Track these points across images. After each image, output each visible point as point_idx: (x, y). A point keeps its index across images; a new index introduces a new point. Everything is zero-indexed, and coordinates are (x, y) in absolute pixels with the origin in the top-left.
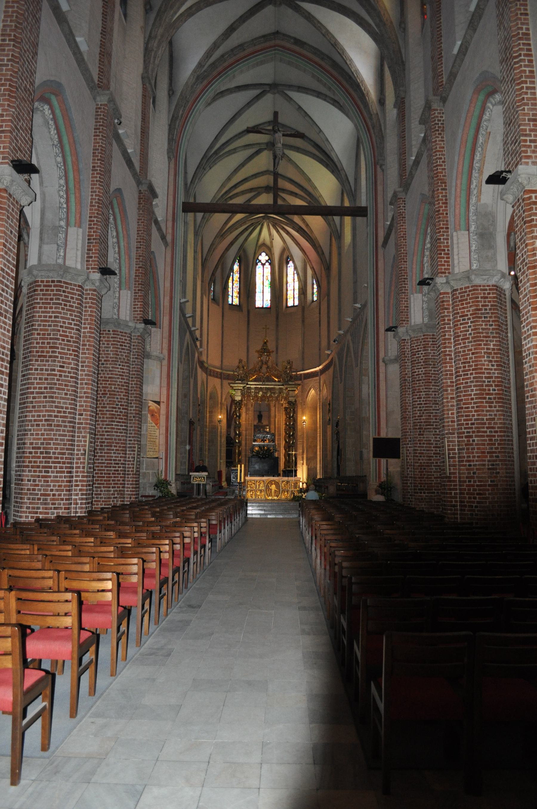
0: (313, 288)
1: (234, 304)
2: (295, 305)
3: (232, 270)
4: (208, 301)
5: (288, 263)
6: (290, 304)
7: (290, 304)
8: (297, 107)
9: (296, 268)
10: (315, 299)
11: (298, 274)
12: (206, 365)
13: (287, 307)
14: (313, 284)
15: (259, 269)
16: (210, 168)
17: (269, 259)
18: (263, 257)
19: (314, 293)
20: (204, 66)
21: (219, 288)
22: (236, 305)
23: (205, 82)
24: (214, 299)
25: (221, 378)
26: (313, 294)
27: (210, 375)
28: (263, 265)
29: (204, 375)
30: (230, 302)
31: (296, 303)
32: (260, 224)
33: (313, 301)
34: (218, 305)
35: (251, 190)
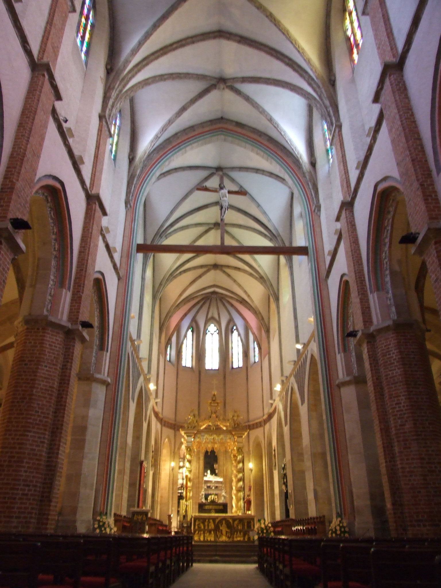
0: (254, 352)
1: (187, 366)
2: (240, 366)
3: (185, 336)
4: (165, 361)
5: (232, 332)
6: (235, 366)
7: (235, 366)
8: (239, 186)
9: (239, 335)
10: (257, 360)
11: (242, 340)
12: (160, 415)
13: (232, 368)
14: (254, 348)
15: (208, 337)
16: (166, 238)
17: (217, 329)
18: (212, 328)
19: (255, 355)
20: (160, 137)
21: (174, 353)
22: (189, 368)
23: (161, 153)
24: (170, 361)
25: (174, 429)
26: (255, 356)
27: (165, 425)
28: (212, 334)
29: (159, 425)
30: (184, 365)
31: (241, 365)
32: (208, 299)
33: (255, 362)
34: (173, 365)
35: (202, 267)
